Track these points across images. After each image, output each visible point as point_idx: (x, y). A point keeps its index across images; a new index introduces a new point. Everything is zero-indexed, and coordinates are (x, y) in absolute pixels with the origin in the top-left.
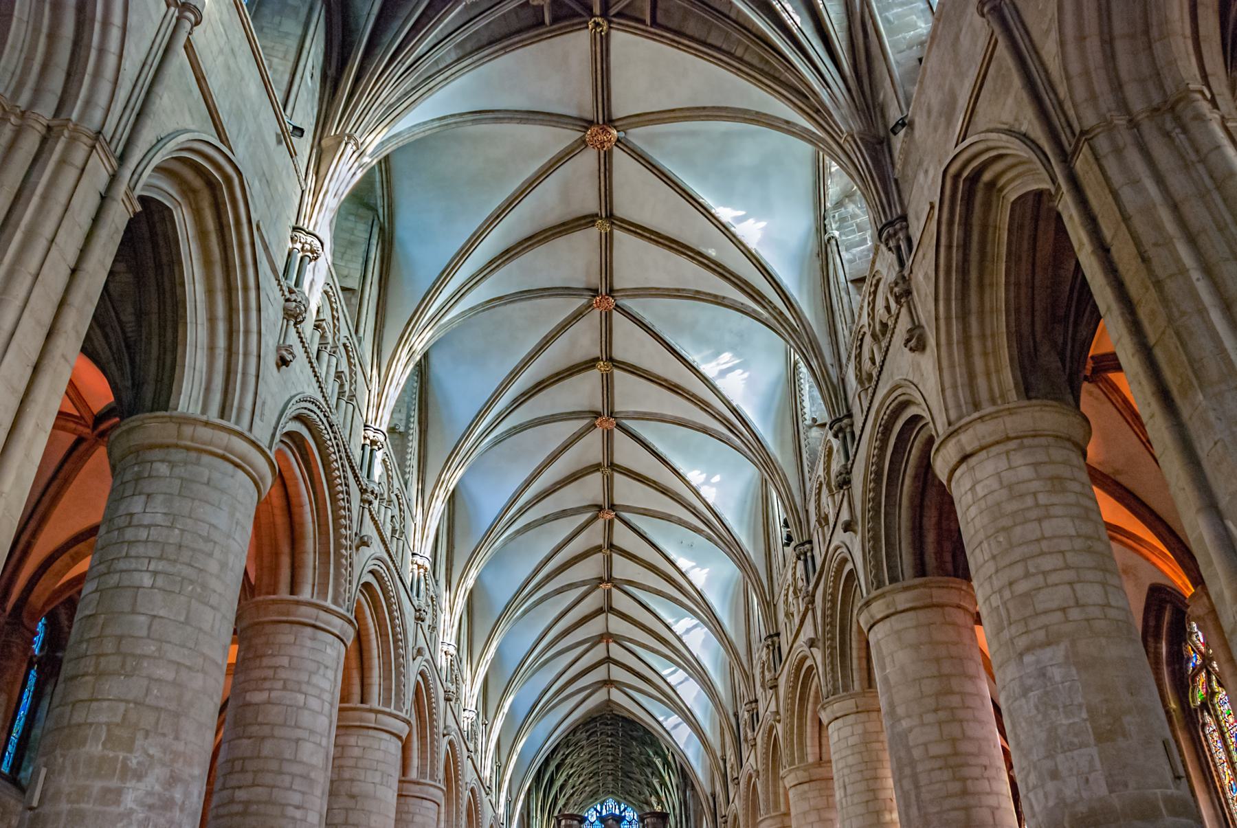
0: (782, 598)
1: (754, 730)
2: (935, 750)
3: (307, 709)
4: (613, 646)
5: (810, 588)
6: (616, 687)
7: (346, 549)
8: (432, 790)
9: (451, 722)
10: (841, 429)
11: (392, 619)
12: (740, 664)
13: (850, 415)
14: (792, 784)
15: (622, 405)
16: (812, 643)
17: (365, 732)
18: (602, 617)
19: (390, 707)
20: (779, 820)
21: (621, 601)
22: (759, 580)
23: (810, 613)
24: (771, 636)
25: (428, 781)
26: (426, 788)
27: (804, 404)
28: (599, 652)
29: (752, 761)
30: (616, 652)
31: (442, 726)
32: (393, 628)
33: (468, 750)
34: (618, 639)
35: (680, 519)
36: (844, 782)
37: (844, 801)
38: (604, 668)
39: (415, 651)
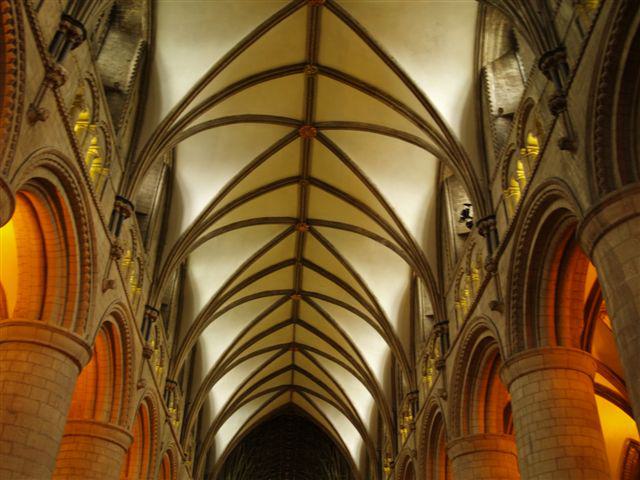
4: (299, 355)
5: (494, 256)
6: (299, 392)
7: (12, 109)
8: (119, 434)
10: (552, 63)
13: (562, 48)
15: (323, 114)
16: (495, 306)
17: (38, 348)
18: (289, 328)
19: (68, 327)
21: (307, 313)
22: (431, 276)
23: (492, 280)
24: (440, 324)
25: (116, 425)
26: (112, 432)
27: (491, 99)
28: (285, 360)
30: (301, 360)
31: (136, 379)
32: (82, 250)
34: (303, 348)
36: (530, 438)
37: (529, 457)
39: (106, 283)
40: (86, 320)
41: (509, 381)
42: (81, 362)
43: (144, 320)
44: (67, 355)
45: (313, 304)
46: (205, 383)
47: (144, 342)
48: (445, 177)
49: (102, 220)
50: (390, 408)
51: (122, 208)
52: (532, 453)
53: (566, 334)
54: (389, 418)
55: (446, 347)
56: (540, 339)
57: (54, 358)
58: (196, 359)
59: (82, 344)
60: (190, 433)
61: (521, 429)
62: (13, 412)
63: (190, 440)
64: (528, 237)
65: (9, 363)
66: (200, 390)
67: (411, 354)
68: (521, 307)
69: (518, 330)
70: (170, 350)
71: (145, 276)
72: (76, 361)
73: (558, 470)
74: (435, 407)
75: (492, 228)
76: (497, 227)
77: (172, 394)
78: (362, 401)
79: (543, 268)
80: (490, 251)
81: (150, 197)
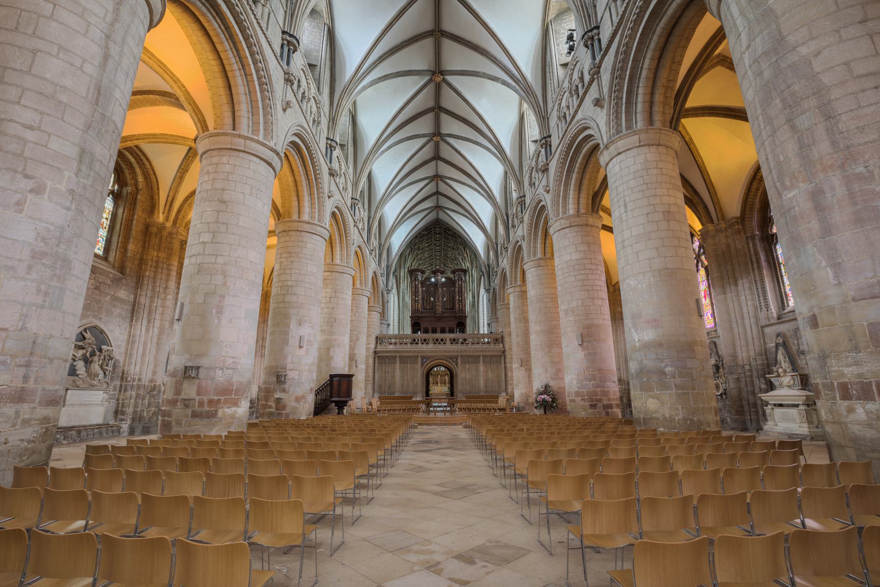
0: (556, 107)
1: (522, 213)
2: (860, 68)
3: (55, 20)
4: (441, 184)
8: (319, 228)
9: (334, 188)
11: (255, 62)
12: (515, 175)
14: (556, 230)
16: (598, 103)
17: (236, 153)
18: (434, 163)
19: (258, 136)
20: (536, 262)
21: (446, 152)
22: (537, 102)
23: (596, 81)
24: (545, 138)
25: (316, 222)
26: (315, 226)
29: (521, 232)
30: (443, 188)
32: (257, 71)
33: (355, 222)
35: (484, 73)
36: (625, 201)
38: (435, 197)
39: (284, 104)
40: (272, 131)
41: (607, 161)
42: (276, 169)
43: (327, 148)
44: (261, 159)
45: (448, 144)
46: (379, 203)
47: (329, 164)
48: (550, 18)
49: (270, 45)
50: (504, 213)
51: (288, 42)
52: (626, 212)
53: (657, 117)
54: (503, 220)
55: (549, 155)
56: (636, 123)
57: (250, 161)
58: (358, 137)
59: (272, 150)
60: (373, 236)
61: (617, 195)
62: (223, 202)
63: (375, 242)
64: (634, 30)
65: (215, 166)
66: (377, 208)
67: (520, 170)
68: (622, 98)
69: (618, 117)
70: (351, 177)
71: (322, 114)
72: (270, 164)
73: (648, 222)
74: (541, 201)
75: (596, 37)
76: (601, 36)
77: (357, 207)
78: (485, 211)
79: (645, 57)
80: (594, 58)
81: (318, 51)
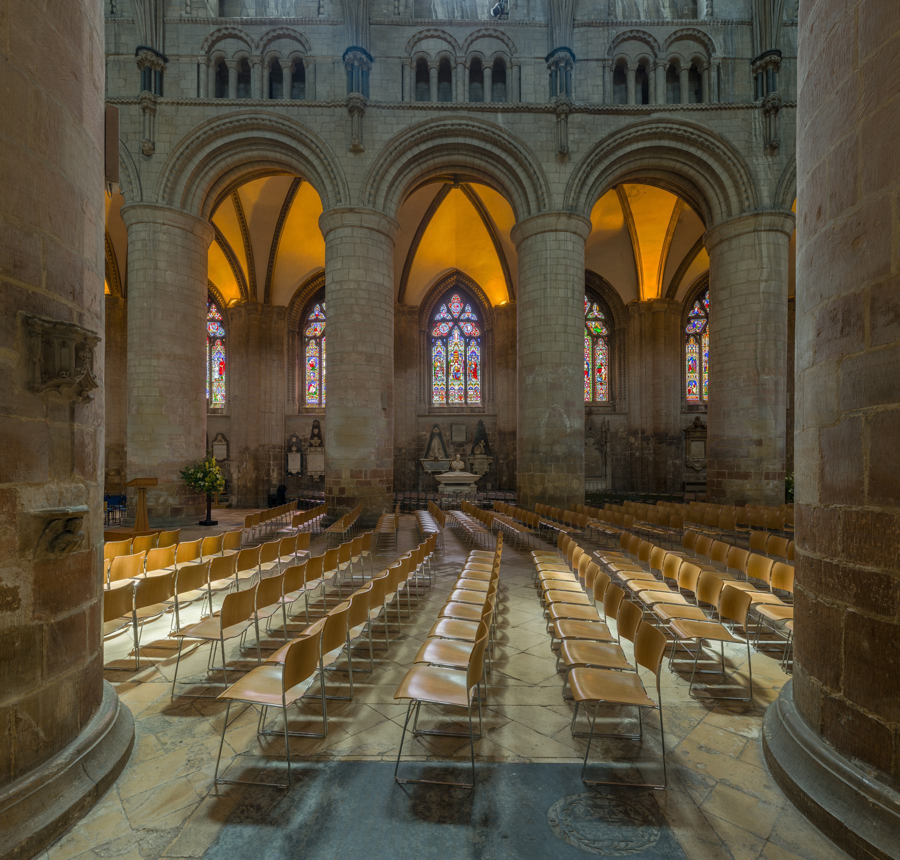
36: (573, 286)
37: (571, 300)
